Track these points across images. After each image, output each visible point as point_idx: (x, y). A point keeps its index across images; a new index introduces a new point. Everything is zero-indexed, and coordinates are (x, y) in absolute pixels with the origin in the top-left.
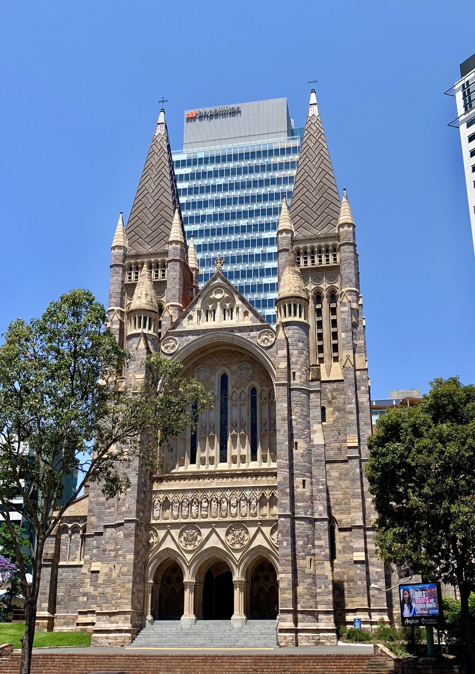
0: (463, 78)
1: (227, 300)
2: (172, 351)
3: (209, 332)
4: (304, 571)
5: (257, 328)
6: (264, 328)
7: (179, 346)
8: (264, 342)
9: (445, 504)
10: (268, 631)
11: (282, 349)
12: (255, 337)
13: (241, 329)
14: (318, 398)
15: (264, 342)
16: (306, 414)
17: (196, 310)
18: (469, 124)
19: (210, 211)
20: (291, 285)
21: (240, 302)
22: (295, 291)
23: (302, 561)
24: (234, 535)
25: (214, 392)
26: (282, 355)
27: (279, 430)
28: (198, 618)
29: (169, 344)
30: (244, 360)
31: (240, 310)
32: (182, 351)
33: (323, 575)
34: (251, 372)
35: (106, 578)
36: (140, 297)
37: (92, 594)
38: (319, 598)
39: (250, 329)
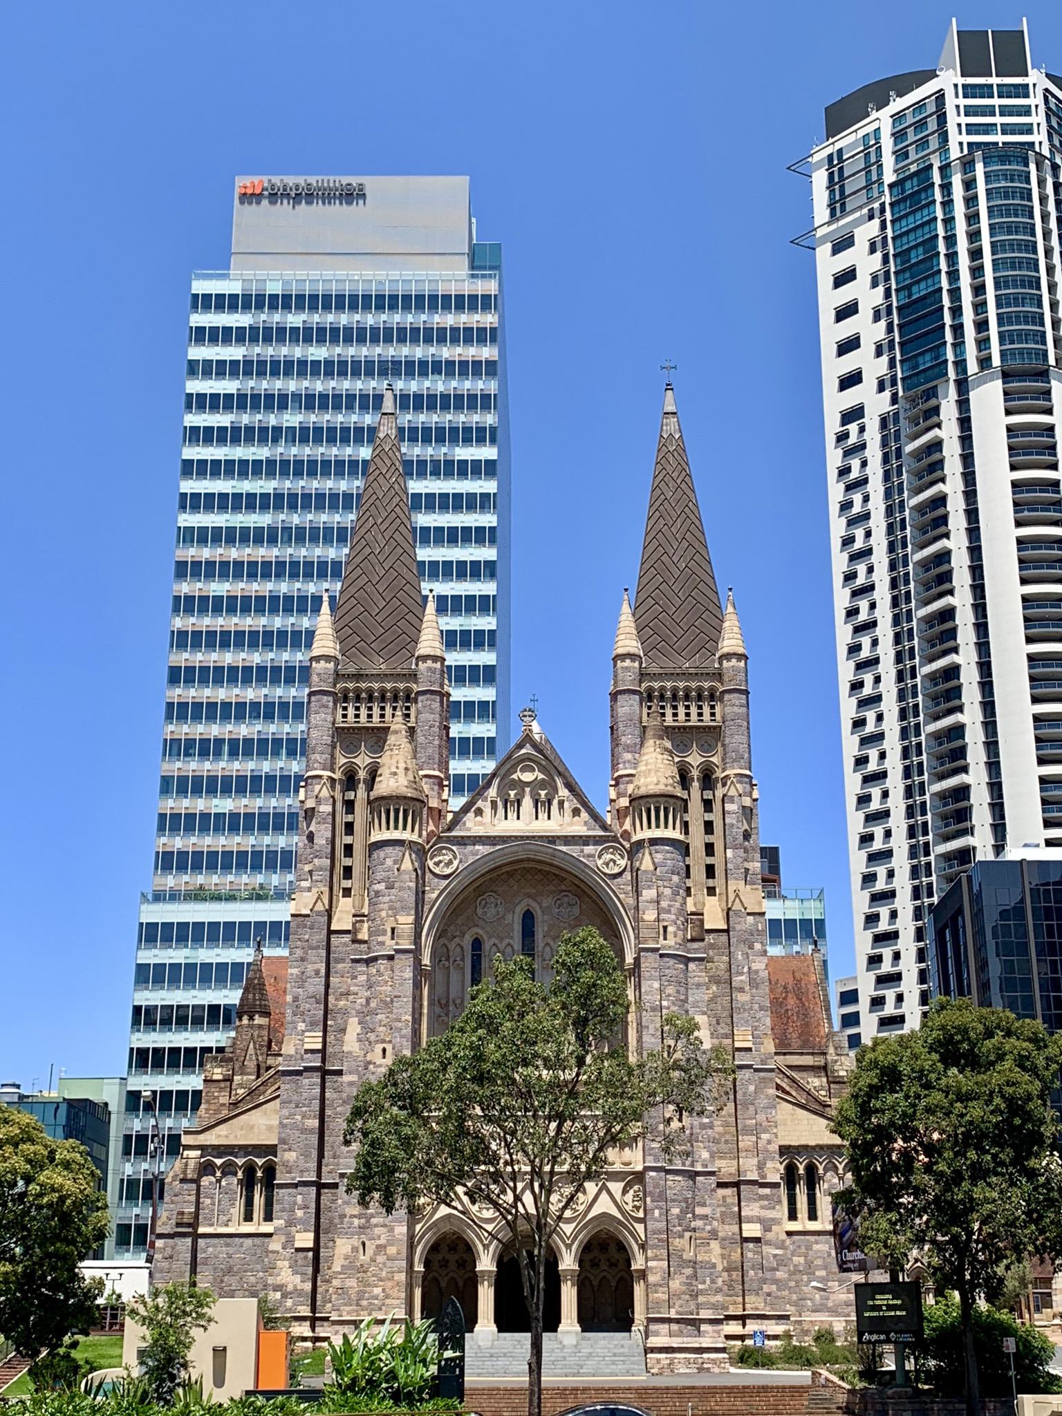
0: (831, 140)
1: (542, 784)
2: (448, 871)
3: (514, 841)
4: (681, 1256)
5: (597, 841)
6: (608, 842)
7: (461, 862)
8: (607, 864)
9: (965, 1185)
10: (622, 1350)
11: (649, 887)
12: (593, 856)
13: (569, 840)
14: (701, 971)
15: (607, 864)
16: (683, 997)
17: (489, 799)
18: (836, 248)
19: (292, 419)
20: (659, 774)
21: (567, 791)
22: (666, 785)
23: (678, 1240)
24: (562, 1195)
25: (511, 942)
26: (648, 898)
27: (647, 1027)
28: (501, 1329)
29: (441, 858)
30: (564, 888)
31: (566, 805)
32: (465, 872)
33: (708, 1262)
34: (576, 911)
35: (346, 1263)
36: (395, 774)
37: (299, 1288)
38: (701, 1299)
39: (585, 840)
